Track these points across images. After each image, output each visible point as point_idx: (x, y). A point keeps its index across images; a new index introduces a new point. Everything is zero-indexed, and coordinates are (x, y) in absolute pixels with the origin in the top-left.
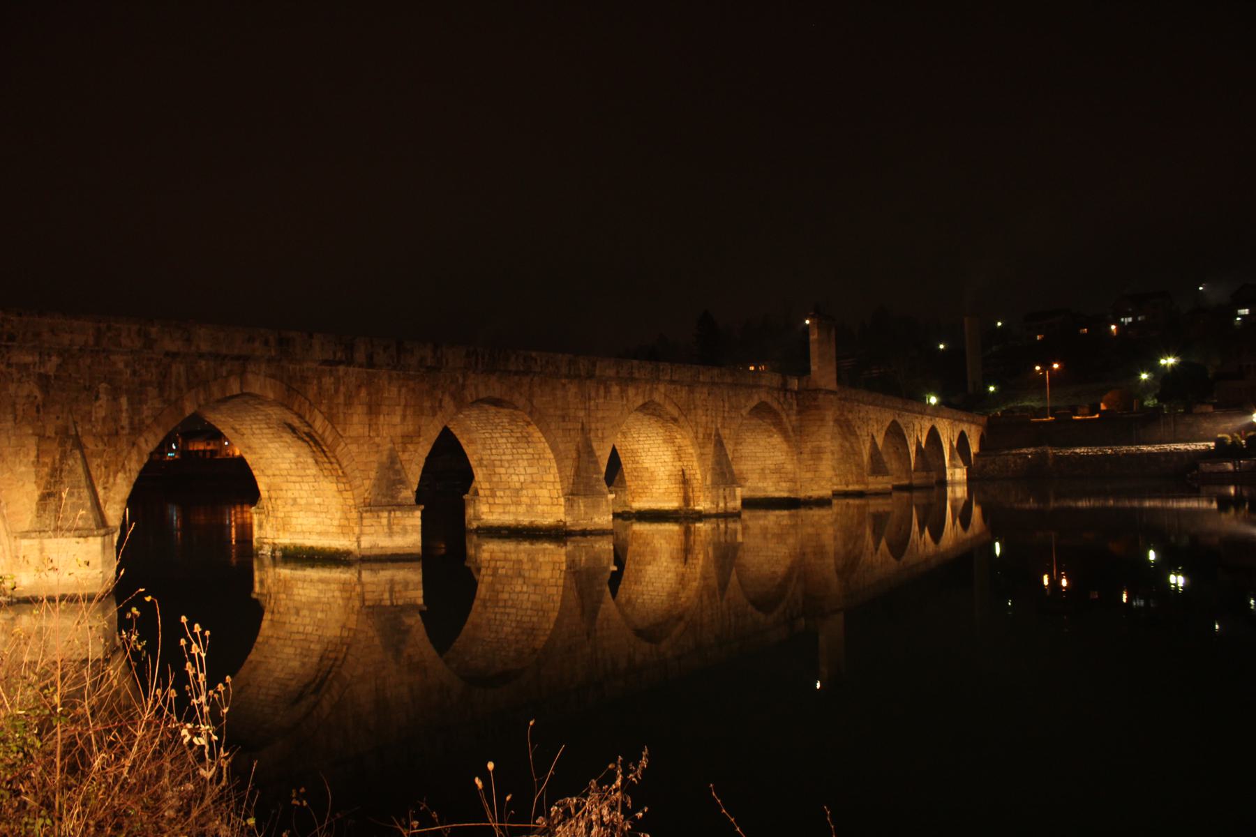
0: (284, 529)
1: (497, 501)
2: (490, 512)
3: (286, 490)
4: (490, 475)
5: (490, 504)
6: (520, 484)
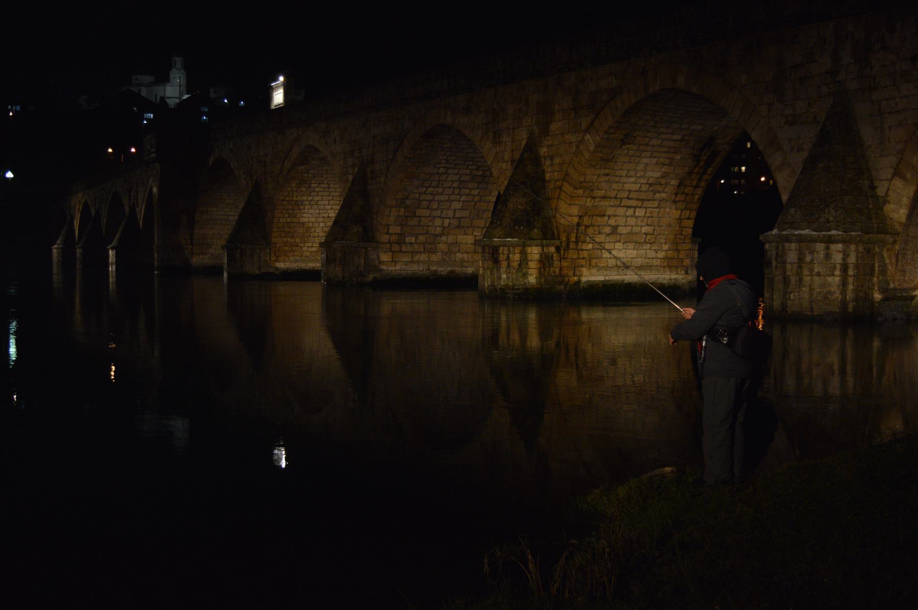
0: (590, 264)
1: (403, 249)
2: (392, 261)
3: (609, 216)
4: (407, 217)
5: (393, 252)
6: (441, 229)
